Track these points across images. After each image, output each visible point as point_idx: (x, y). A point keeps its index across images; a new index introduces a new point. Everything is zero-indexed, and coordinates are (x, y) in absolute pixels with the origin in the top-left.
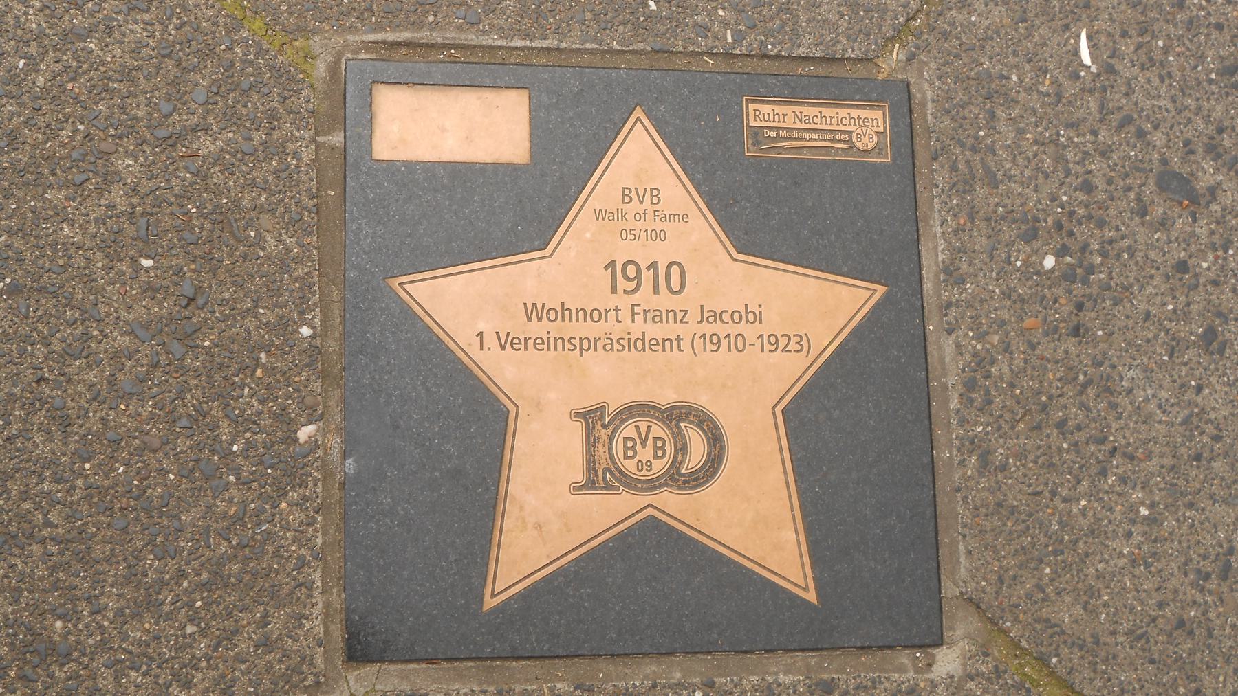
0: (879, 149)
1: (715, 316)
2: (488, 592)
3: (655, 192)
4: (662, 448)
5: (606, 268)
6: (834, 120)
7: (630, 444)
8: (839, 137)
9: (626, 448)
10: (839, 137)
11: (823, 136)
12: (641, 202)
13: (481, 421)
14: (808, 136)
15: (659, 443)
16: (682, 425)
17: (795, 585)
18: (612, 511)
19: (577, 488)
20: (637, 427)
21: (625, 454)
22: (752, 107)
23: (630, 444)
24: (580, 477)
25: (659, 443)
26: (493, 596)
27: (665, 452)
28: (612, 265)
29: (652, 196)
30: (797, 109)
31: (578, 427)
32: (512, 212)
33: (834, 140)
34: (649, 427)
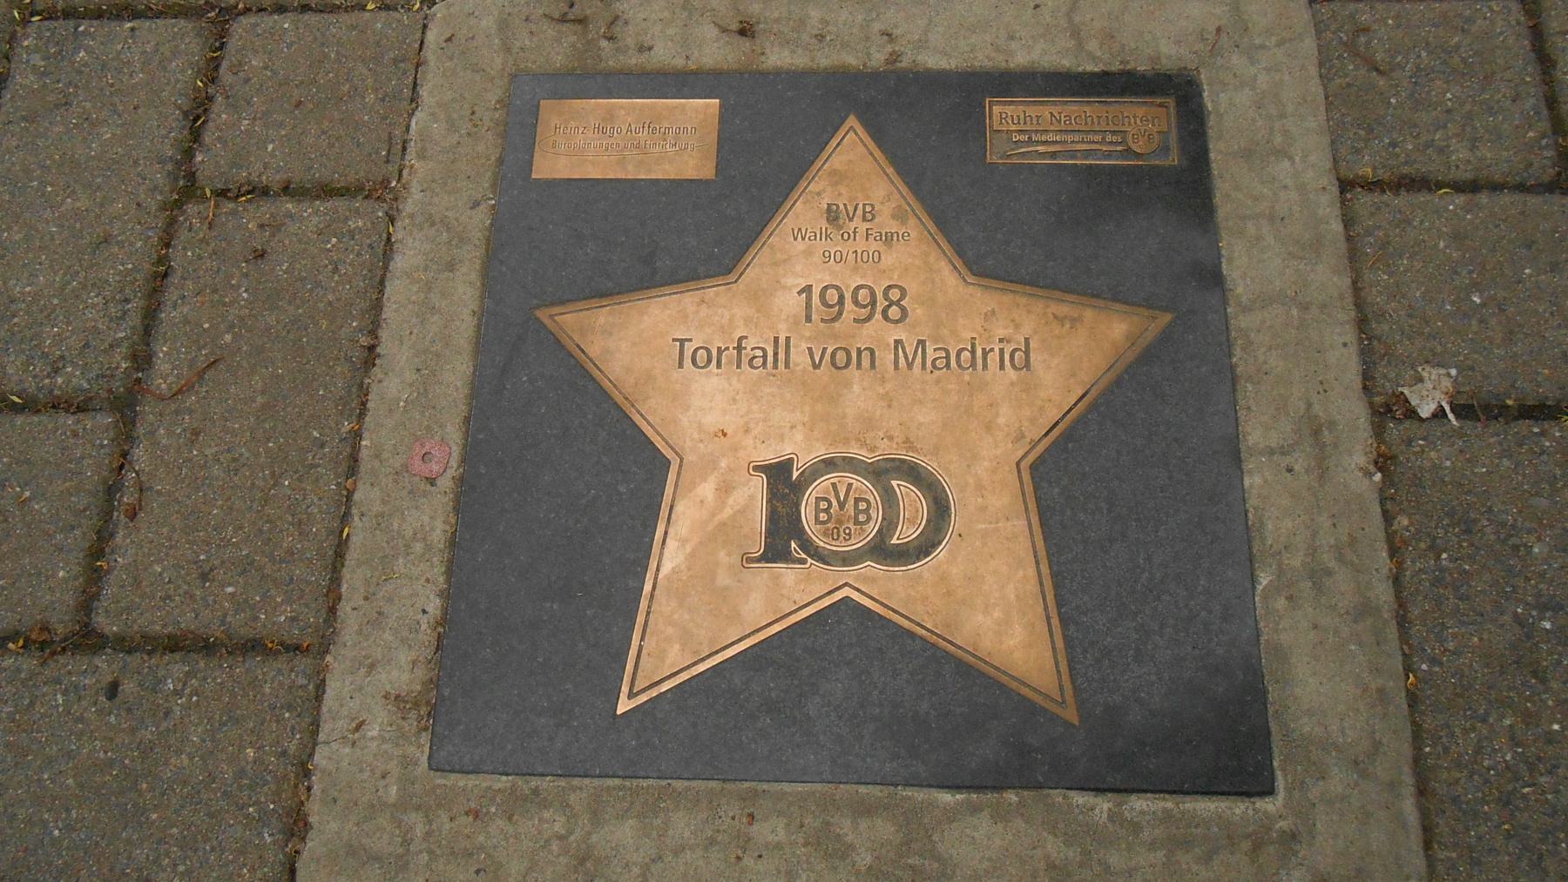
0: (1164, 149)
1: (948, 357)
2: (625, 689)
3: (868, 209)
4: (866, 511)
5: (799, 293)
6: (1103, 123)
7: (823, 505)
8: (1109, 138)
9: (818, 511)
10: (1109, 138)
11: (1091, 137)
12: (851, 220)
13: (629, 473)
14: (1069, 138)
15: (862, 506)
16: (894, 483)
17: (1052, 700)
18: (798, 590)
19: (750, 560)
20: (834, 485)
21: (817, 518)
22: (996, 109)
23: (823, 505)
24: (758, 548)
25: (862, 506)
26: (631, 695)
27: (869, 519)
28: (807, 289)
29: (864, 212)
30: (1055, 110)
31: (759, 484)
32: (696, 235)
33: (1103, 142)
34: (850, 485)
